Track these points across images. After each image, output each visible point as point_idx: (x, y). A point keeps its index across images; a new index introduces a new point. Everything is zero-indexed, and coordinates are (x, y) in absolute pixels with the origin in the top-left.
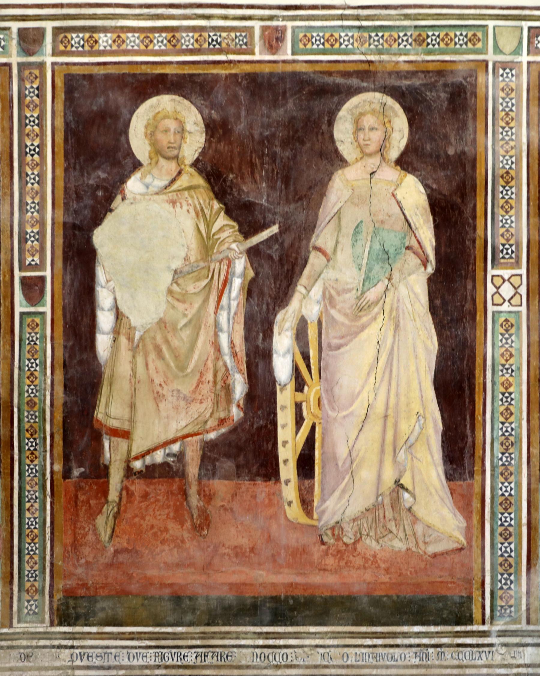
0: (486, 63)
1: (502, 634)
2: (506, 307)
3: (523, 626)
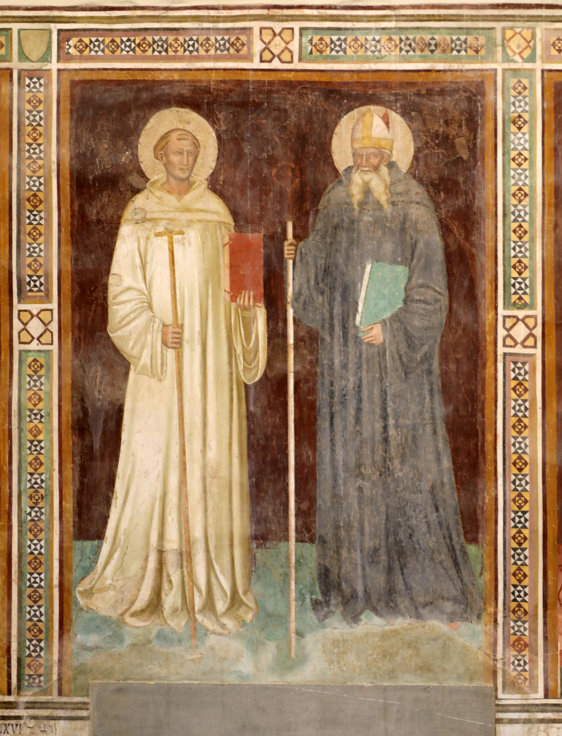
0: (10, 71)
1: (31, 705)
2: (34, 345)
3: (55, 697)
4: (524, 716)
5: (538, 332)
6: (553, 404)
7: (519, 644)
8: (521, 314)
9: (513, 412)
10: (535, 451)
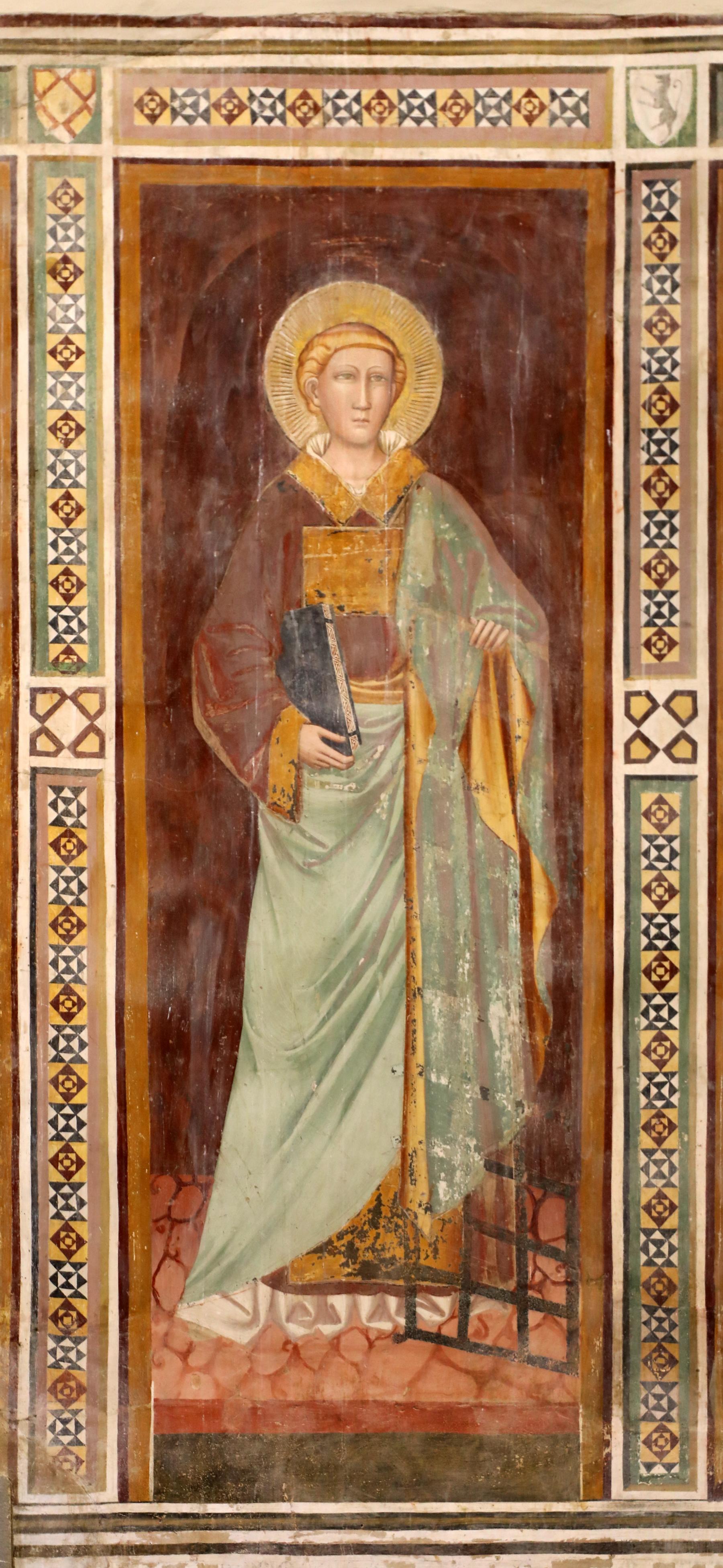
4: (76, 1539)
5: (107, 722)
6: (141, 879)
7: (65, 1388)
8: (70, 684)
9: (52, 894)
10: (99, 976)
